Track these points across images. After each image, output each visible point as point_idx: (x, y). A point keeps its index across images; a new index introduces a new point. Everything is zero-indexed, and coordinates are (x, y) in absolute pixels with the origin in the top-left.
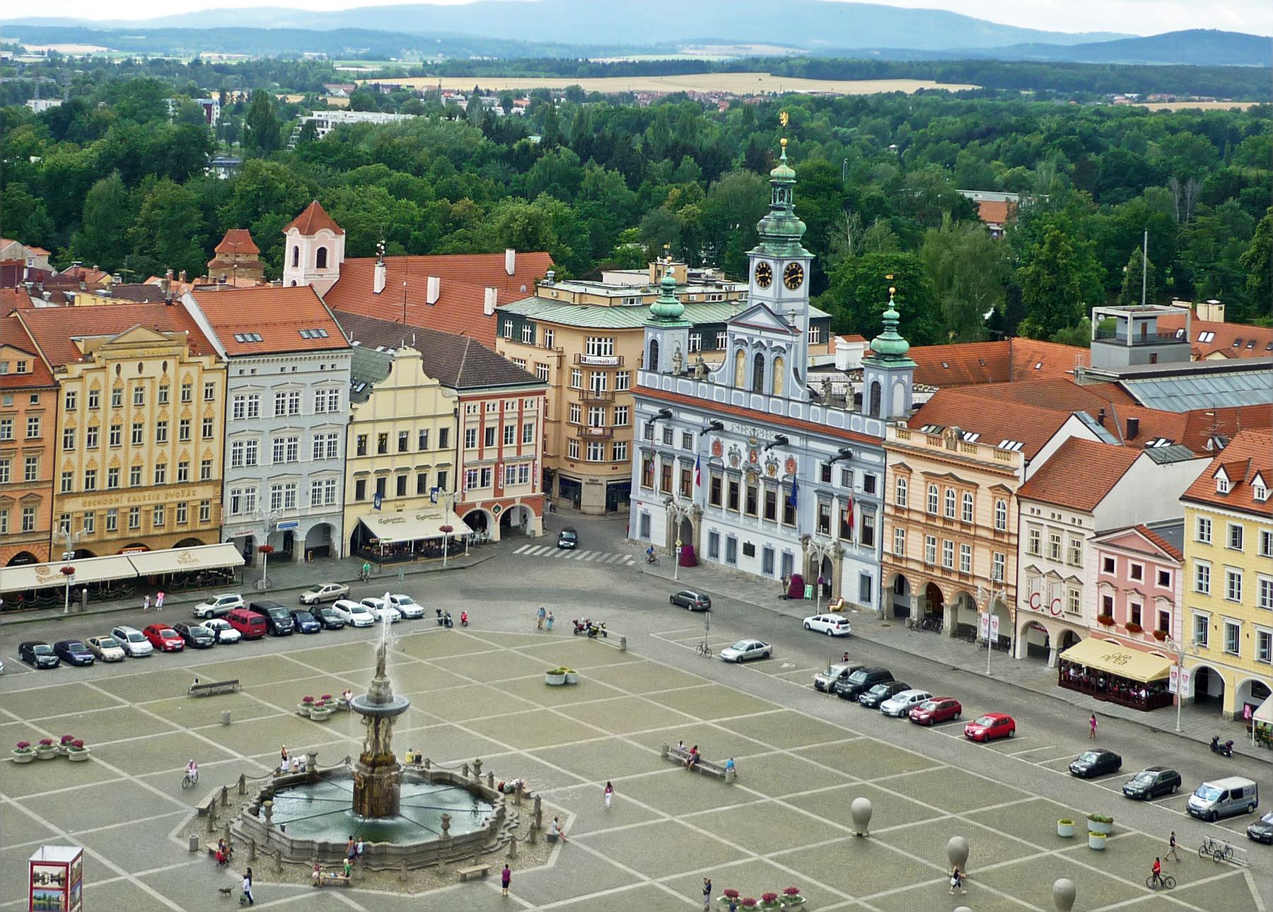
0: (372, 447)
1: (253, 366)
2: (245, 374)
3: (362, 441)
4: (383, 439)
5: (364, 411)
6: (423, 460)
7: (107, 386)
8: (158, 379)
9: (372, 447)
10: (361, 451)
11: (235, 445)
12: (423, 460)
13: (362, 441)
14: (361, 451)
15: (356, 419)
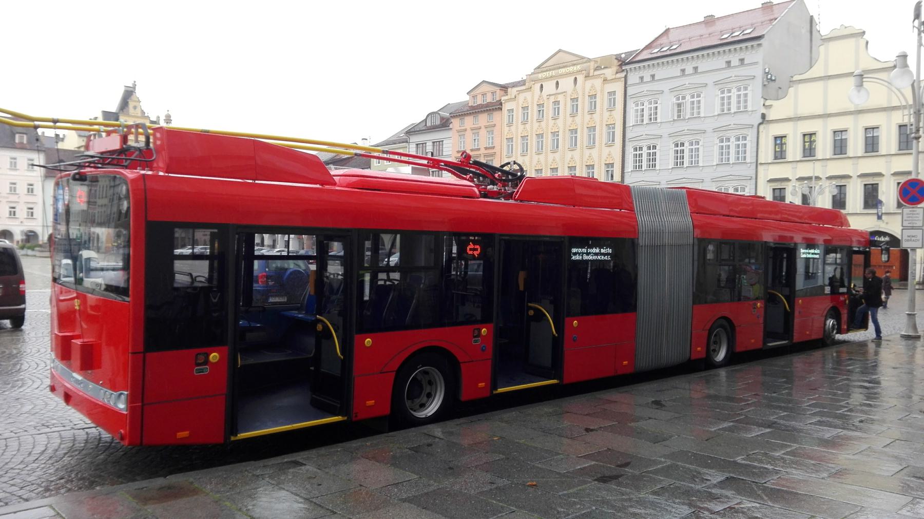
0: (794, 149)
1: (651, 72)
2: (645, 80)
3: (780, 140)
4: (809, 138)
5: (778, 109)
6: (871, 165)
7: (533, 103)
8: (569, 93)
9: (794, 149)
10: (780, 155)
11: (636, 149)
12: (871, 165)
13: (780, 140)
14: (780, 155)
15: (770, 117)
